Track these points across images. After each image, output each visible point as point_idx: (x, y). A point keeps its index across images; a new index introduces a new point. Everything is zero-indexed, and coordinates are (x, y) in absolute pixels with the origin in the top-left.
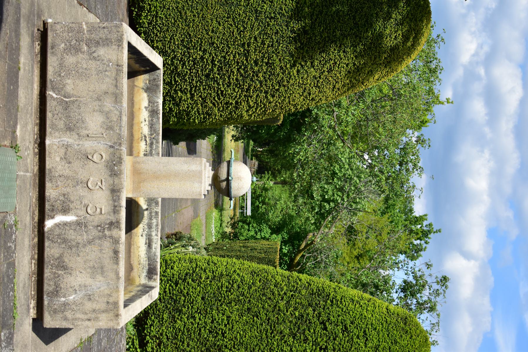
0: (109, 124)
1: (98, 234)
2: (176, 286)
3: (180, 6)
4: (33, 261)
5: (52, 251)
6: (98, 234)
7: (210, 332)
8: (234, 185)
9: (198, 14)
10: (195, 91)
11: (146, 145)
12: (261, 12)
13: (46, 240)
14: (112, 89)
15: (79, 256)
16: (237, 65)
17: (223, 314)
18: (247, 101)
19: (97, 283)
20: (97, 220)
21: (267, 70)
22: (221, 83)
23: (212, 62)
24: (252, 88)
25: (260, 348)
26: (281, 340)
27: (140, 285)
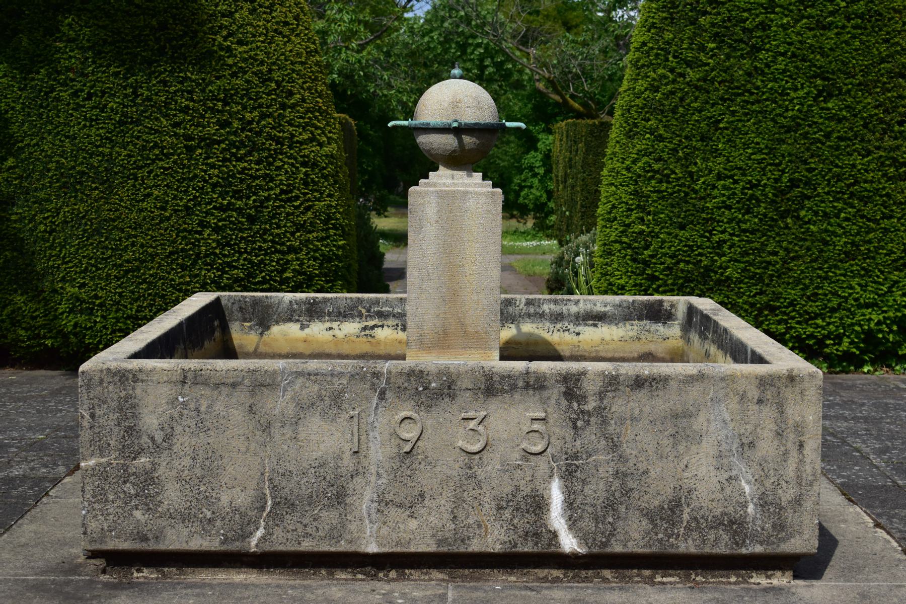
0: (327, 401)
1: (593, 428)
2: (658, 279)
3: (114, 272)
4: (658, 579)
5: (635, 535)
6: (593, 428)
7: (748, 212)
8: (470, 117)
9: (130, 236)
10: (283, 244)
11: (382, 326)
12: (125, 115)
13: (608, 550)
14: (242, 396)
15: (646, 472)
16: (230, 160)
17: (714, 187)
18: (301, 143)
19: (712, 427)
20: (560, 430)
21: (239, 104)
22: (266, 194)
23: (225, 211)
24: (274, 132)
25: (780, 115)
26: (763, 74)
27: (685, 336)
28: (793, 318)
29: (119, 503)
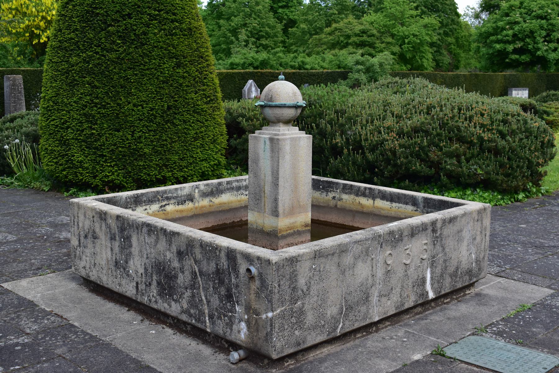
11: (169, 204)
13: (441, 294)
28: (175, 169)
29: (289, 329)
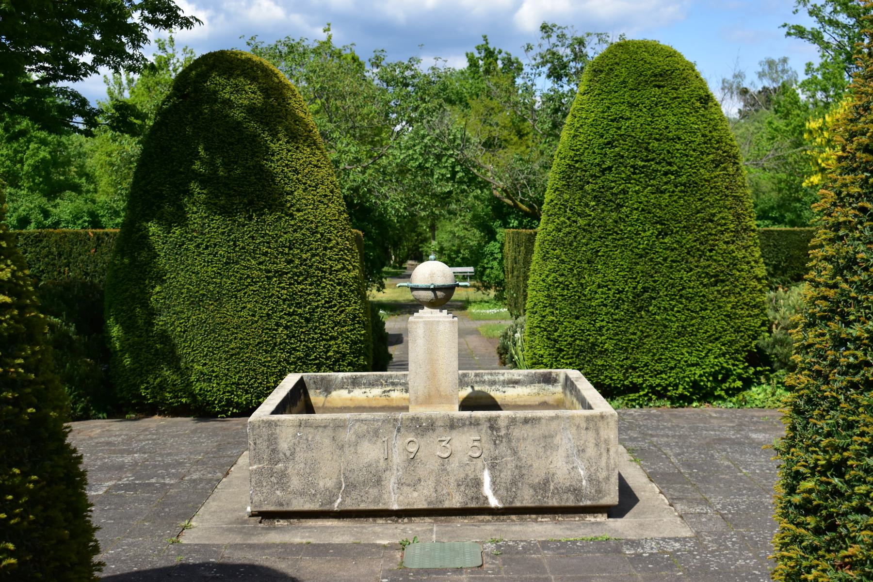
0: (372, 434)
1: (504, 444)
2: (563, 350)
3: (224, 356)
4: (540, 519)
5: (527, 497)
6: (504, 444)
7: (617, 308)
8: (440, 282)
9: (233, 333)
10: (327, 335)
12: (229, 258)
13: (514, 505)
14: (329, 432)
15: (531, 466)
16: (293, 284)
17: (596, 293)
18: (337, 271)
19: (563, 442)
20: (487, 445)
21: (298, 248)
22: (316, 304)
23: (291, 316)
24: (320, 265)
25: (636, 247)
26: (625, 221)
27: (564, 393)
28: (647, 374)
29: (268, 487)
